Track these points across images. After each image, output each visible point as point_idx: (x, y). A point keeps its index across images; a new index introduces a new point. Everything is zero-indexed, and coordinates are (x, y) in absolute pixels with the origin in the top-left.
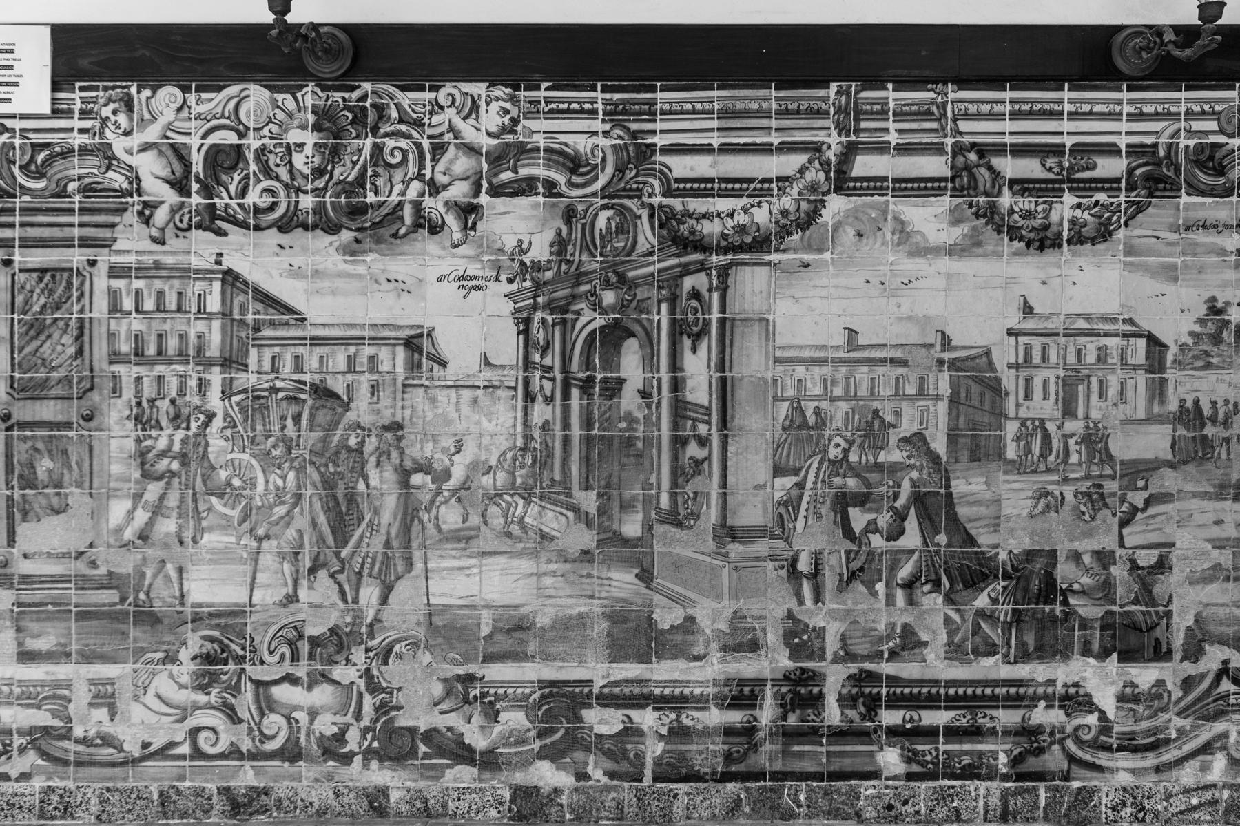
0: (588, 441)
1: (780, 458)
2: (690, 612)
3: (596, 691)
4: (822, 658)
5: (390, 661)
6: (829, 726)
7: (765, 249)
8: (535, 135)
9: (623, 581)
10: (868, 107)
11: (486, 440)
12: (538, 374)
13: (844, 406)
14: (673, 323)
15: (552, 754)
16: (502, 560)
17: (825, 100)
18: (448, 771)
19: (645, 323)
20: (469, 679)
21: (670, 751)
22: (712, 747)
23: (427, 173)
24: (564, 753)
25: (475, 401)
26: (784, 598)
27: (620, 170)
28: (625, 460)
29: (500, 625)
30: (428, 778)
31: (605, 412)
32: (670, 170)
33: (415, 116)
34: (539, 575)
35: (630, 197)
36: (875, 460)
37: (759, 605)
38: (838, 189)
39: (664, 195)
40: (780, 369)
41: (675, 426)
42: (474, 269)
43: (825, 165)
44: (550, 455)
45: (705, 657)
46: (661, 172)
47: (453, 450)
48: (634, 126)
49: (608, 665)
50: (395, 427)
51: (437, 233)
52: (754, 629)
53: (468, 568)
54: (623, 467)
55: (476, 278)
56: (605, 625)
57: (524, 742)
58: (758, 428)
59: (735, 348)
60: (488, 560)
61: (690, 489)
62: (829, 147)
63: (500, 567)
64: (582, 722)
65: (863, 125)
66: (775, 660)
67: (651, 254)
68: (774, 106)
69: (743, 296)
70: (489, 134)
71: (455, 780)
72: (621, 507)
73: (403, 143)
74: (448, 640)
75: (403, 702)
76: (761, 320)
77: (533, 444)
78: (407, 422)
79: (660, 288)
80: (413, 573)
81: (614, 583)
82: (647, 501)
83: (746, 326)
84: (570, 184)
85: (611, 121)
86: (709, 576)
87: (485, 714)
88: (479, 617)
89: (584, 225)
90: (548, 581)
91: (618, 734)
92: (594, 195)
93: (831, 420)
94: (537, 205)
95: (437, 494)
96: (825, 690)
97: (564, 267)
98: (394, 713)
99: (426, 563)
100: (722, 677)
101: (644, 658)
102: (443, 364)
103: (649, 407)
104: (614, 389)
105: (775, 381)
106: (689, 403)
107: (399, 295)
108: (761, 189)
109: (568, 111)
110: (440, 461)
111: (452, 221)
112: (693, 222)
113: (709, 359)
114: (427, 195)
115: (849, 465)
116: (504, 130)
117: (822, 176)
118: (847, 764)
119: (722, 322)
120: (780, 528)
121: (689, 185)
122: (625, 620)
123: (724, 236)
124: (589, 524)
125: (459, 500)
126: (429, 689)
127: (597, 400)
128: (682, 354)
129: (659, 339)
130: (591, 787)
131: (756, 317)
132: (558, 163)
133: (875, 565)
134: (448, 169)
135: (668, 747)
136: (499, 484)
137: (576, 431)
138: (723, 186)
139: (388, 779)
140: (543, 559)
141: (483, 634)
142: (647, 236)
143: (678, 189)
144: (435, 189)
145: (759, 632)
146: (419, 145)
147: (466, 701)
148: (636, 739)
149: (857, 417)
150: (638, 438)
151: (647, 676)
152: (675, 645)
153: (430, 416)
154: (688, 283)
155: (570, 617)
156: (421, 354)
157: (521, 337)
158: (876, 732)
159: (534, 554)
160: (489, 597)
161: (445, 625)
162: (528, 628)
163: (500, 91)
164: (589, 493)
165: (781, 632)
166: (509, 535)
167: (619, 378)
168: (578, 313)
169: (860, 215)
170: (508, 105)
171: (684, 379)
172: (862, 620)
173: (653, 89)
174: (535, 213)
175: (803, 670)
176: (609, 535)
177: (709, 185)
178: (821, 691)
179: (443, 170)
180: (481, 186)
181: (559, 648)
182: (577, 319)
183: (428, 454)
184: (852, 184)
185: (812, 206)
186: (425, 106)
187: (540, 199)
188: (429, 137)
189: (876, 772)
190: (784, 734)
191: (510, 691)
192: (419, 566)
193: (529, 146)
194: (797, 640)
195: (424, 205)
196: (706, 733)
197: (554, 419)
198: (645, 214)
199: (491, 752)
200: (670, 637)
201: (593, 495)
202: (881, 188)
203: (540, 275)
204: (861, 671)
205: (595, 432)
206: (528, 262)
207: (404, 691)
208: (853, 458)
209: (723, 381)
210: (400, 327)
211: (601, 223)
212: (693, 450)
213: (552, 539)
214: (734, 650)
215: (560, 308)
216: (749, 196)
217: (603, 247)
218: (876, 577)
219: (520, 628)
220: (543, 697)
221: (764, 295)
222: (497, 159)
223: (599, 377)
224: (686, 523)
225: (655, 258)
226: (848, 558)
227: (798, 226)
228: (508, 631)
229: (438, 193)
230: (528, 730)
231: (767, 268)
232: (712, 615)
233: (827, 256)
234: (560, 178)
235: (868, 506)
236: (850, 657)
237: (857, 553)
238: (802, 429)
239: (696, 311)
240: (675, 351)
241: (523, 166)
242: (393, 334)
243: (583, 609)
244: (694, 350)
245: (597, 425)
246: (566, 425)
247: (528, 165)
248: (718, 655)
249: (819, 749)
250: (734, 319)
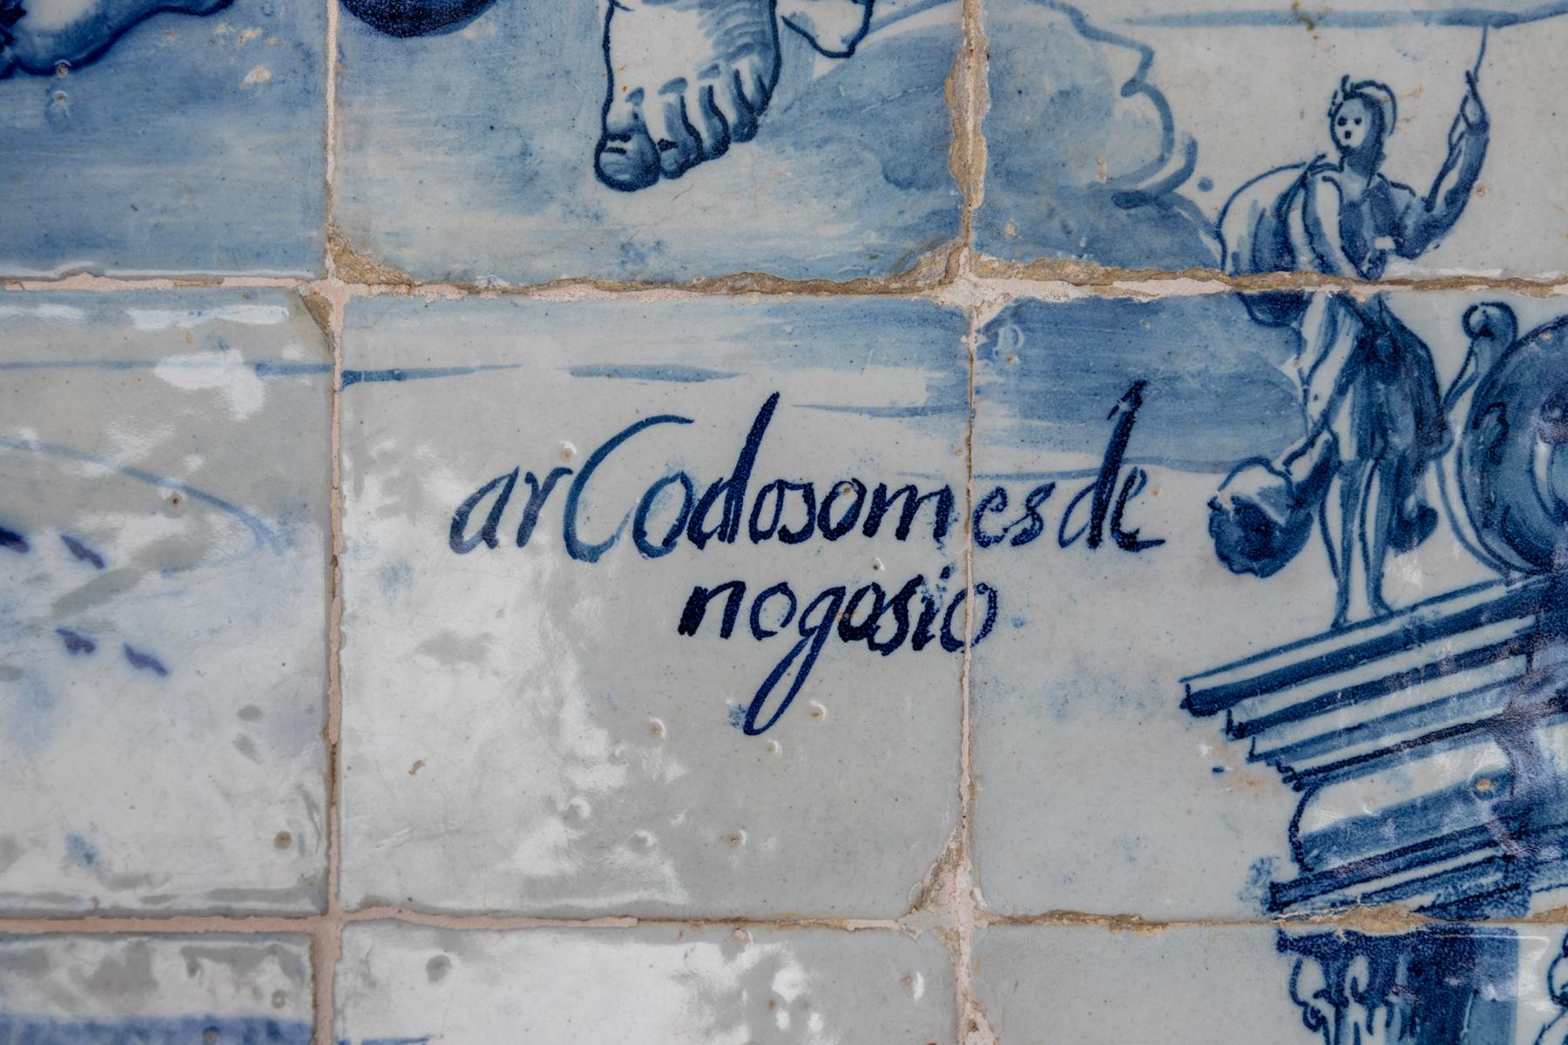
42: (853, 415)
55: (874, 508)
206: (1438, 325)
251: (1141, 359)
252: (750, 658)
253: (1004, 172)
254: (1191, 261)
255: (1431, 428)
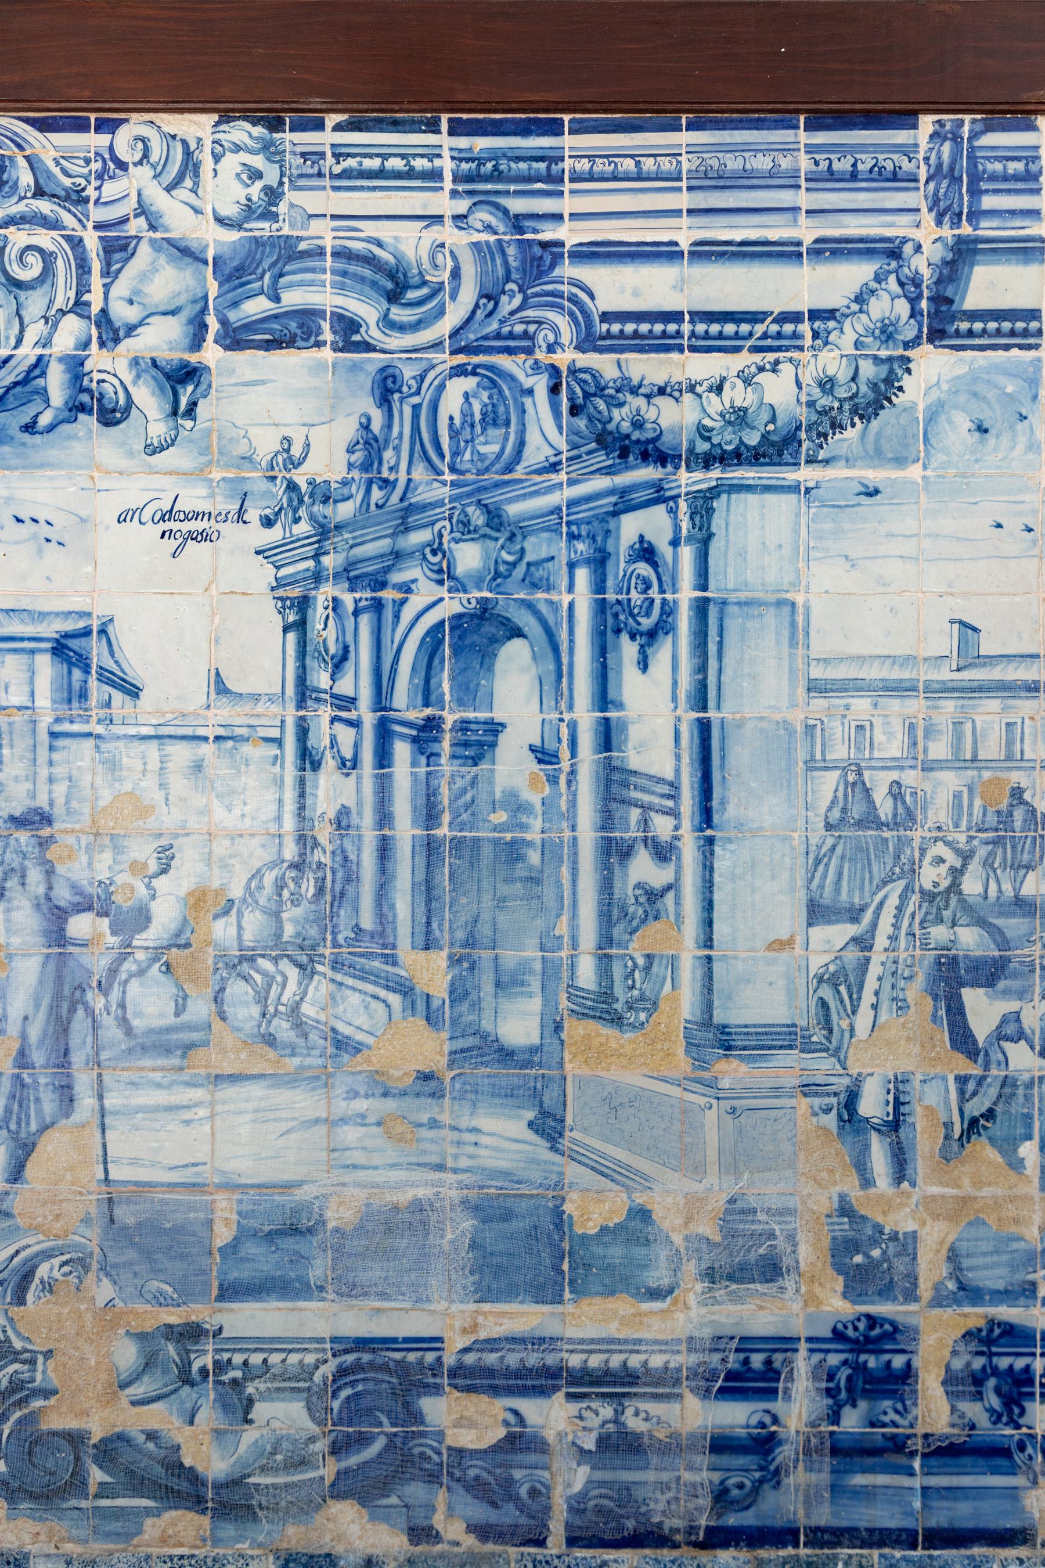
0: (430, 848)
1: (822, 887)
2: (640, 1199)
3: (449, 1359)
4: (911, 1295)
5: (30, 1297)
6: (926, 1436)
7: (786, 457)
8: (314, 222)
9: (501, 1136)
10: (998, 167)
11: (221, 847)
12: (325, 713)
13: (951, 781)
14: (601, 607)
15: (359, 1488)
16: (255, 1090)
17: (908, 151)
18: (149, 1522)
19: (543, 608)
20: (191, 1334)
21: (601, 1484)
22: (687, 1476)
23: (95, 299)
24: (384, 1487)
25: (198, 767)
26: (831, 1172)
27: (490, 296)
28: (504, 889)
29: (253, 1223)
30: (108, 1535)
31: (463, 791)
32: (592, 297)
33: (67, 182)
34: (333, 1123)
35: (510, 351)
36: (1017, 891)
37: (782, 1187)
38: (937, 335)
39: (579, 348)
40: (819, 703)
41: (606, 821)
43: (911, 285)
44: (351, 878)
45: (670, 1291)
46: (573, 299)
47: (153, 867)
48: (517, 205)
49: (473, 1306)
50: (36, 819)
51: (118, 423)
52: (772, 1235)
53: (188, 1107)
54: (500, 903)
55: (197, 515)
56: (468, 1224)
57: (303, 1463)
58: (773, 819)
59: (725, 661)
60: (228, 1092)
61: (636, 949)
62: (918, 248)
63: (250, 1106)
64: (422, 1423)
65: (988, 202)
66: (811, 1302)
67: (554, 467)
68: (805, 163)
69: (743, 554)
70: (220, 220)
71: (164, 1541)
72: (498, 984)
73: (45, 239)
74: (148, 1255)
75: (55, 1382)
76: (779, 603)
77: (317, 856)
78: (58, 811)
79: (572, 537)
80: (76, 1118)
81: (484, 1140)
82: (549, 973)
83: (747, 617)
84: (388, 324)
85: (471, 193)
86: (677, 1127)
87: (225, 1406)
88: (210, 1207)
89: (416, 408)
90: (350, 1134)
91: (495, 1449)
92: (436, 345)
93: (924, 809)
94: (320, 367)
95: (123, 957)
96: (917, 1362)
97: (376, 494)
98: (37, 1403)
99: (101, 1097)
100: (707, 1333)
101: (547, 1292)
102: (133, 691)
103: (553, 780)
104: (481, 744)
105: (810, 729)
106: (634, 773)
107: (40, 551)
108: (779, 335)
109: (380, 174)
110: (129, 889)
111: (148, 399)
112: (640, 402)
113: (675, 683)
114: (95, 345)
115: (963, 902)
116: (249, 210)
117: (903, 308)
118: (961, 1514)
119: (701, 608)
120: (823, 1029)
121: (630, 328)
122: (507, 1216)
123: (703, 432)
124: (432, 1019)
125: (168, 968)
126: (108, 1354)
127: (446, 766)
128: (619, 673)
129: (571, 641)
130: (442, 1556)
131: (772, 598)
132: (362, 280)
133: (1017, 1107)
134: (137, 292)
135: (598, 1475)
136: (248, 937)
137: (405, 829)
138: (701, 328)
139: (27, 1538)
140: (340, 1090)
141: (219, 1243)
142: (545, 431)
143: (609, 335)
144: (111, 332)
145: (781, 1242)
146: (76, 243)
147: (186, 1379)
148: (533, 1458)
149: (978, 803)
150: (530, 844)
151: (553, 1329)
152: (610, 1268)
153: (106, 796)
154: (631, 527)
155: (396, 1208)
156: (86, 670)
157: (291, 636)
158: (1022, 1447)
159: (321, 1080)
160: (232, 1166)
161: (140, 1225)
162: (310, 1231)
163: (242, 132)
164: (432, 954)
165: (826, 1242)
166: (270, 1040)
167: (490, 722)
168: (407, 588)
169: (981, 388)
170: (258, 161)
171: (623, 725)
172: (991, 1219)
173: (555, 129)
174: (315, 382)
175: (872, 1321)
176: (472, 1041)
177: (672, 328)
178: (908, 1364)
179: (127, 294)
180: (204, 326)
181: (374, 1272)
182: (403, 602)
183: (103, 874)
184: (964, 326)
185: (883, 371)
186: (88, 161)
187: (327, 354)
188: (98, 227)
189: (1023, 1531)
190: (835, 1451)
191: (275, 1359)
192: (86, 1103)
193: (303, 246)
194: (858, 1259)
195: (88, 366)
196: (674, 1447)
197: (360, 804)
198: (541, 384)
199: (236, 1482)
200: (599, 1250)
201: (440, 959)
202: (1025, 333)
203: (328, 510)
204: (992, 1323)
205: (443, 831)
207: (59, 1358)
208: (971, 885)
209: (704, 728)
210: (42, 616)
211: (452, 404)
212: (643, 869)
213: (358, 1048)
214: (731, 1278)
215: (370, 578)
216: (756, 349)
217: (456, 453)
218: (1020, 1131)
219: (294, 1231)
220: (342, 1372)
221: (786, 551)
222: (236, 274)
223: (450, 718)
224: (631, 1017)
225: (563, 476)
226: (962, 1092)
227: (855, 411)
228: (270, 1236)
229: (117, 340)
230: (312, 1439)
231: (792, 497)
232: (684, 1205)
233: (915, 472)
234: (367, 310)
235: (1001, 984)
236: (969, 1292)
237: (981, 1081)
238: (867, 821)
239: (648, 586)
240: (604, 666)
241: (290, 286)
242: (29, 630)
243: (422, 1193)
244: (644, 664)
245: (446, 818)
246: (384, 818)
247: (301, 284)
248: (699, 1287)
249: (905, 1481)
250: (724, 603)
251: (247, 488)
252: (173, 544)
253: (221, 453)
254: (256, 470)
255: (301, 501)
